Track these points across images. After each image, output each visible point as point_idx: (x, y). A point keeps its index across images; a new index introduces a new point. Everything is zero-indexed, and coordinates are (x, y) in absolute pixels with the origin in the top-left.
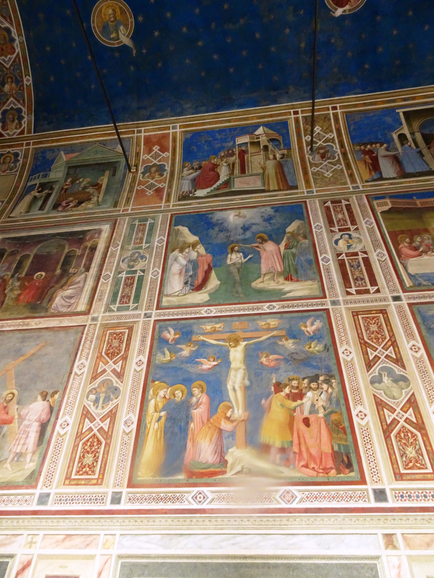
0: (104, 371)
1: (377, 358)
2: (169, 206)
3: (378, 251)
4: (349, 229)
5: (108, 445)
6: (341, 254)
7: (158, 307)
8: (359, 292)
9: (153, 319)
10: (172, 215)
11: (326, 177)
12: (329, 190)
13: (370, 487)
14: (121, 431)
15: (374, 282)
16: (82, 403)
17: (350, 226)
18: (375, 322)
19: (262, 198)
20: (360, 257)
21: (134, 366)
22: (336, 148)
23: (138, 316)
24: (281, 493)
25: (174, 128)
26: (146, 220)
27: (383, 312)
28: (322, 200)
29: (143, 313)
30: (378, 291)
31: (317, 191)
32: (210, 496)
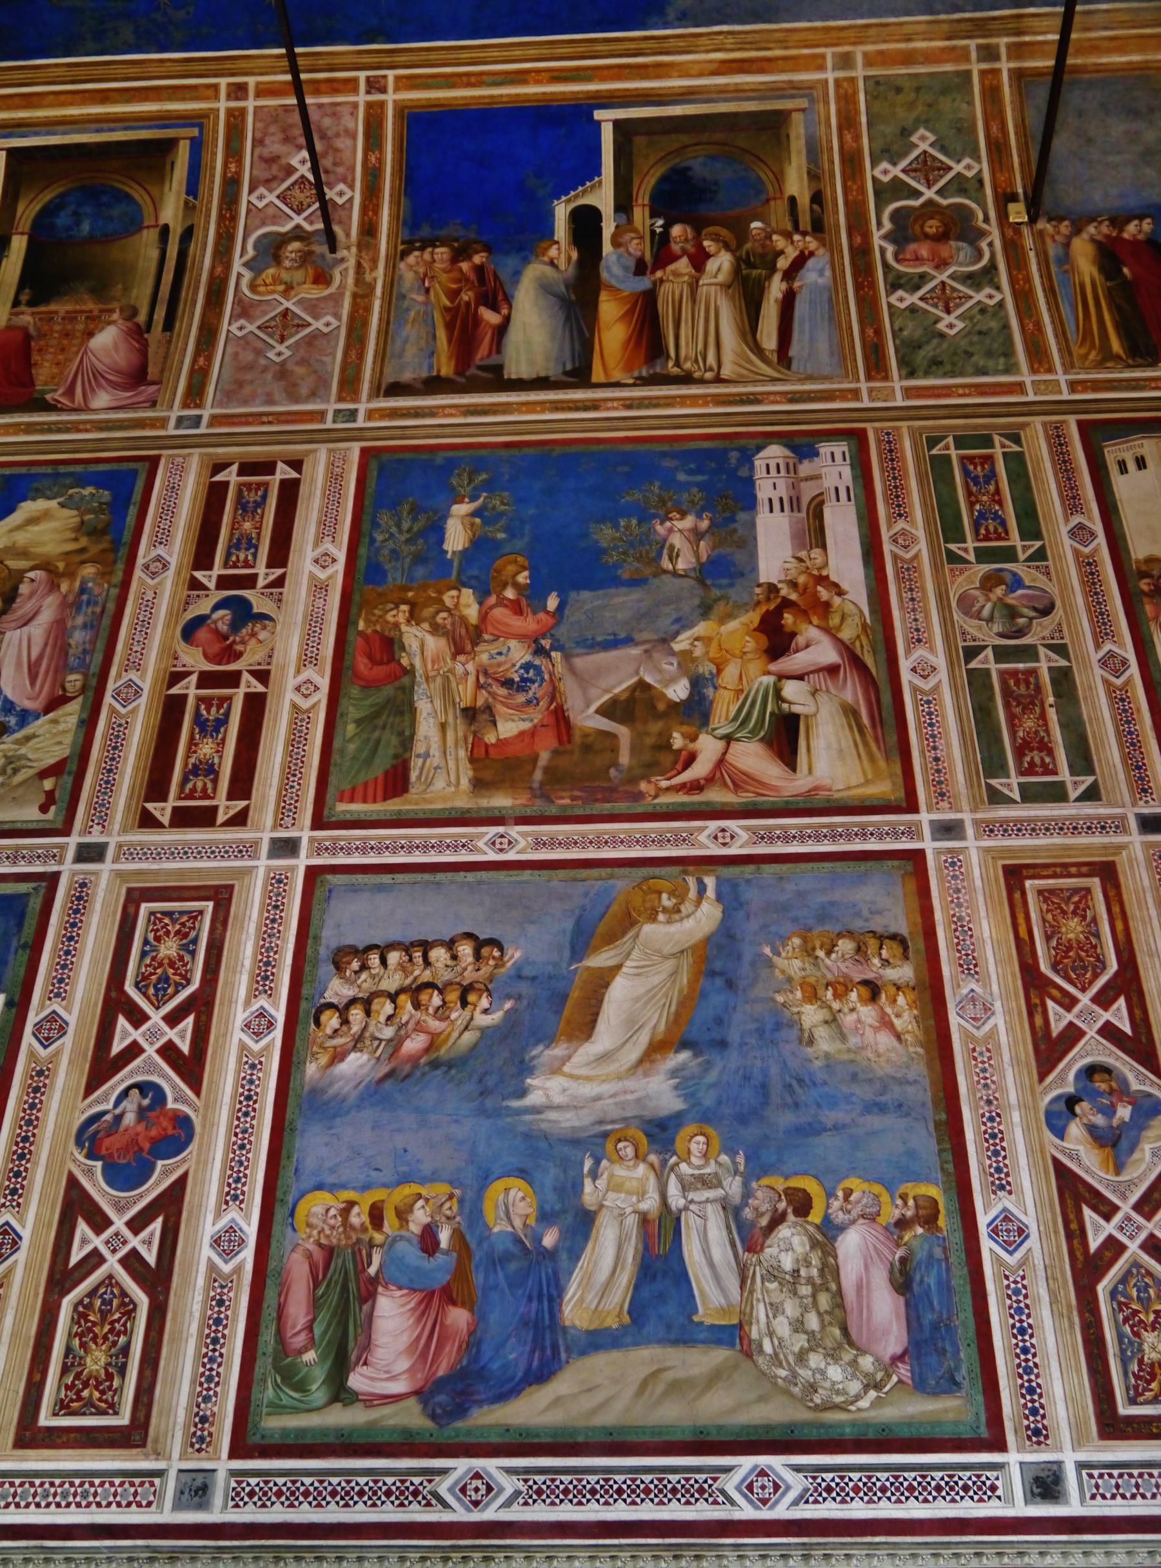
0: (134, 1050)
1: (1073, 1034)
2: (352, 415)
3: (1108, 646)
4: (1009, 555)
5: (158, 1312)
6: (979, 649)
7: (318, 823)
8: (1030, 795)
9: (302, 861)
10: (364, 451)
11: (942, 335)
12: (947, 391)
13: (1017, 1458)
14: (203, 1268)
15: (1083, 760)
16: (63, 1162)
17: (1015, 539)
18: (1076, 908)
19: (706, 404)
20: (1043, 667)
21: (238, 1035)
22: (986, 220)
23: (248, 850)
24: (737, 1477)
25: (375, 86)
26: (268, 467)
27: (1108, 873)
28: (922, 430)
29: (266, 837)
30: (1092, 794)
31: (908, 393)
32: (510, 1485)
